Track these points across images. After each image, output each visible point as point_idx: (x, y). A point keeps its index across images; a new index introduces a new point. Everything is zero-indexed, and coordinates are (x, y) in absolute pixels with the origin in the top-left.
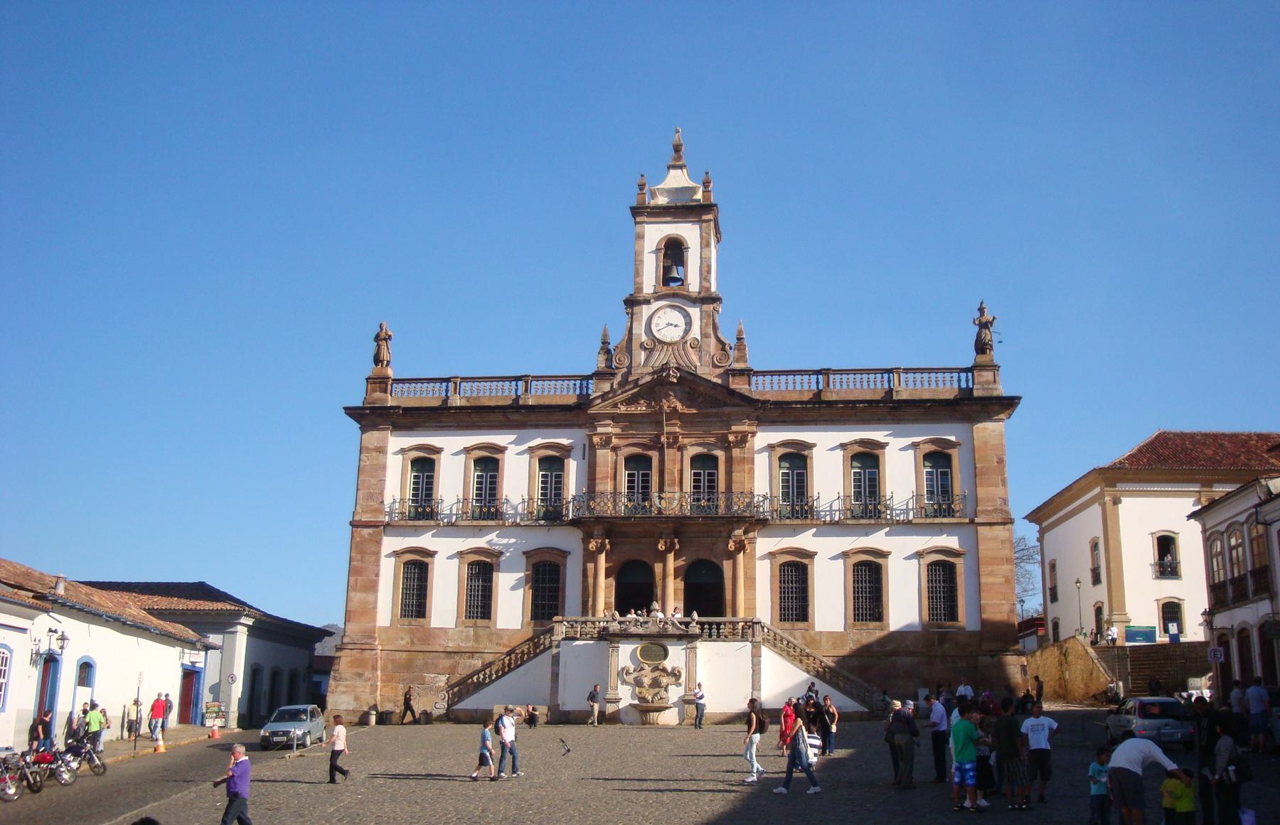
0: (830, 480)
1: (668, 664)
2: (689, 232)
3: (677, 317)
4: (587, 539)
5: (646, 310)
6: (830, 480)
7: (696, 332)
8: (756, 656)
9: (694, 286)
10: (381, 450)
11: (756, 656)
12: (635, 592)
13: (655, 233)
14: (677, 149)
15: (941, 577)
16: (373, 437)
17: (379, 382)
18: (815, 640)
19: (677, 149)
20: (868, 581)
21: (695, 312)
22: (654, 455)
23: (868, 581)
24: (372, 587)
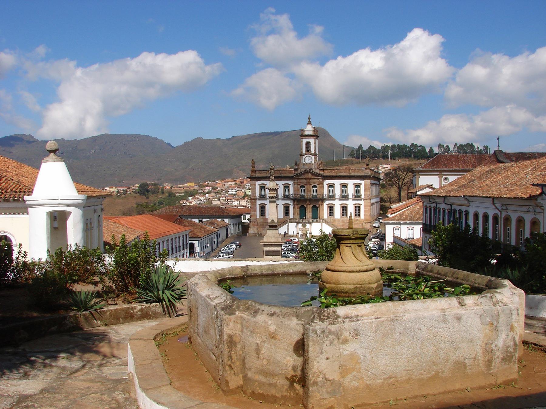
0: (338, 191)
1: (307, 227)
2: (312, 140)
3: (309, 158)
4: (294, 202)
5: (304, 157)
6: (338, 191)
7: (313, 162)
8: (322, 225)
9: (313, 152)
10: (255, 185)
11: (322, 225)
12: (303, 214)
13: (305, 141)
14: (309, 119)
15: (357, 209)
16: (253, 182)
17: (254, 171)
18: (334, 220)
19: (309, 119)
20: (344, 209)
21: (313, 157)
22: (306, 186)
23: (344, 209)
24: (255, 211)
